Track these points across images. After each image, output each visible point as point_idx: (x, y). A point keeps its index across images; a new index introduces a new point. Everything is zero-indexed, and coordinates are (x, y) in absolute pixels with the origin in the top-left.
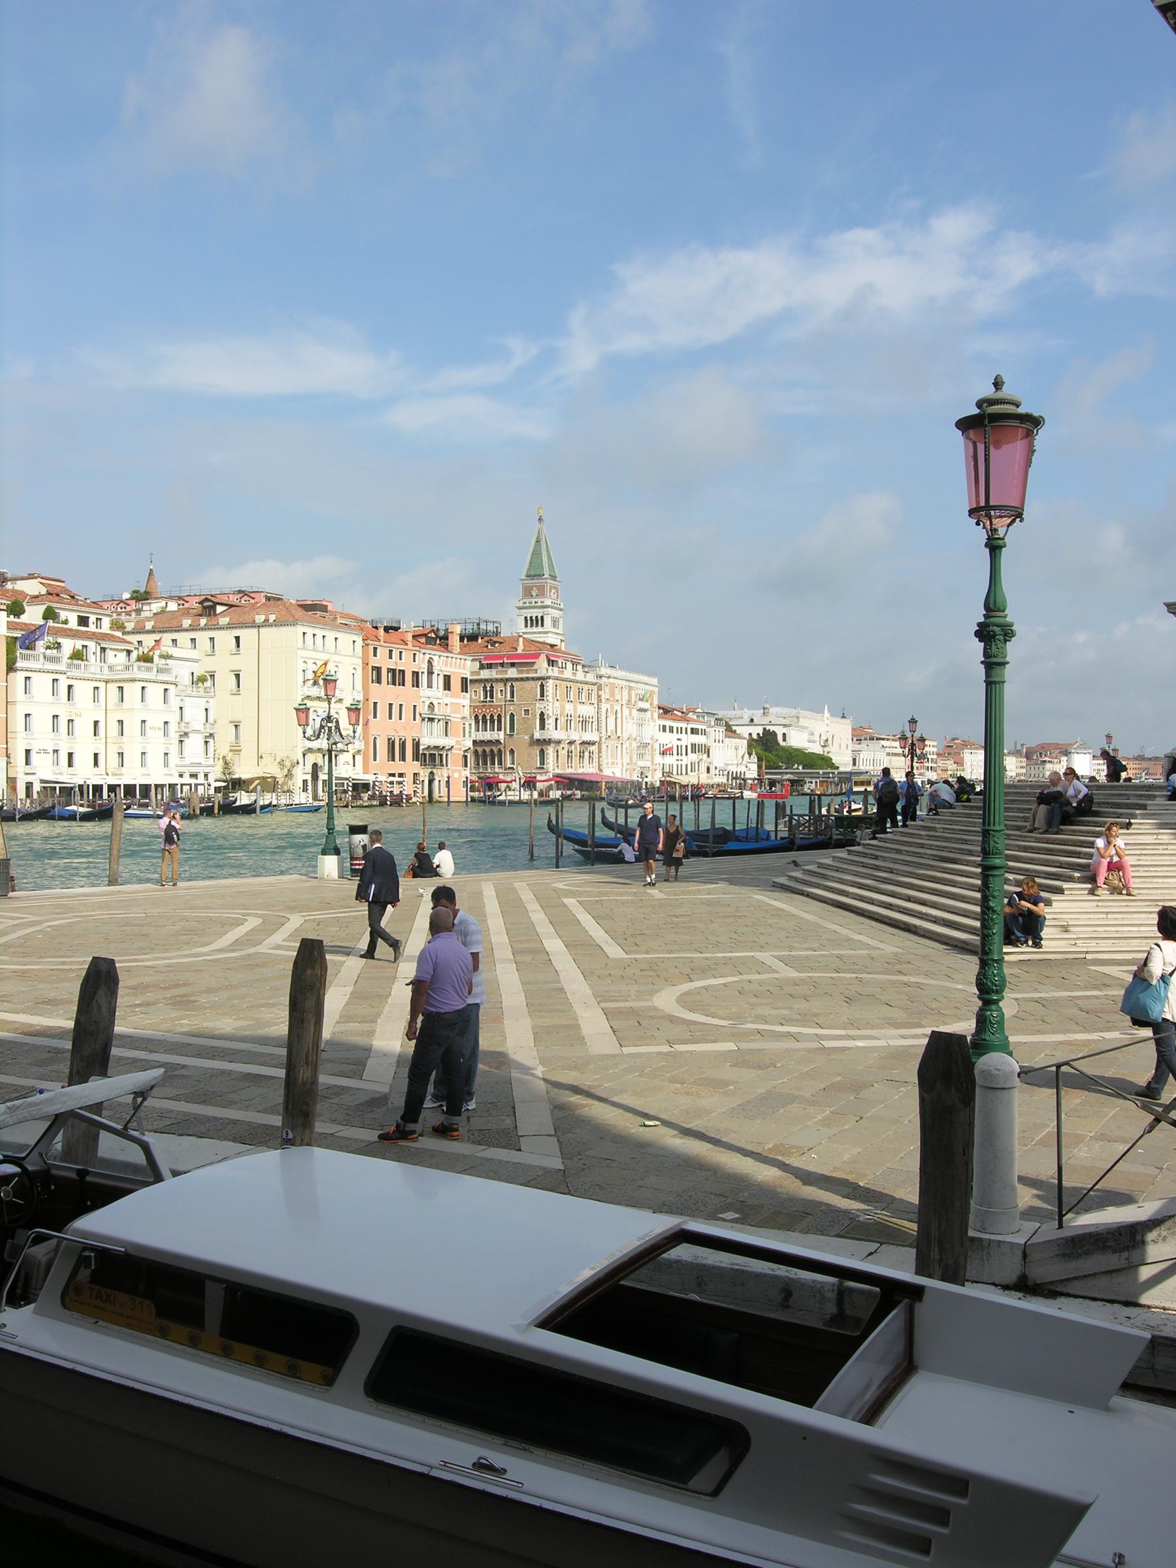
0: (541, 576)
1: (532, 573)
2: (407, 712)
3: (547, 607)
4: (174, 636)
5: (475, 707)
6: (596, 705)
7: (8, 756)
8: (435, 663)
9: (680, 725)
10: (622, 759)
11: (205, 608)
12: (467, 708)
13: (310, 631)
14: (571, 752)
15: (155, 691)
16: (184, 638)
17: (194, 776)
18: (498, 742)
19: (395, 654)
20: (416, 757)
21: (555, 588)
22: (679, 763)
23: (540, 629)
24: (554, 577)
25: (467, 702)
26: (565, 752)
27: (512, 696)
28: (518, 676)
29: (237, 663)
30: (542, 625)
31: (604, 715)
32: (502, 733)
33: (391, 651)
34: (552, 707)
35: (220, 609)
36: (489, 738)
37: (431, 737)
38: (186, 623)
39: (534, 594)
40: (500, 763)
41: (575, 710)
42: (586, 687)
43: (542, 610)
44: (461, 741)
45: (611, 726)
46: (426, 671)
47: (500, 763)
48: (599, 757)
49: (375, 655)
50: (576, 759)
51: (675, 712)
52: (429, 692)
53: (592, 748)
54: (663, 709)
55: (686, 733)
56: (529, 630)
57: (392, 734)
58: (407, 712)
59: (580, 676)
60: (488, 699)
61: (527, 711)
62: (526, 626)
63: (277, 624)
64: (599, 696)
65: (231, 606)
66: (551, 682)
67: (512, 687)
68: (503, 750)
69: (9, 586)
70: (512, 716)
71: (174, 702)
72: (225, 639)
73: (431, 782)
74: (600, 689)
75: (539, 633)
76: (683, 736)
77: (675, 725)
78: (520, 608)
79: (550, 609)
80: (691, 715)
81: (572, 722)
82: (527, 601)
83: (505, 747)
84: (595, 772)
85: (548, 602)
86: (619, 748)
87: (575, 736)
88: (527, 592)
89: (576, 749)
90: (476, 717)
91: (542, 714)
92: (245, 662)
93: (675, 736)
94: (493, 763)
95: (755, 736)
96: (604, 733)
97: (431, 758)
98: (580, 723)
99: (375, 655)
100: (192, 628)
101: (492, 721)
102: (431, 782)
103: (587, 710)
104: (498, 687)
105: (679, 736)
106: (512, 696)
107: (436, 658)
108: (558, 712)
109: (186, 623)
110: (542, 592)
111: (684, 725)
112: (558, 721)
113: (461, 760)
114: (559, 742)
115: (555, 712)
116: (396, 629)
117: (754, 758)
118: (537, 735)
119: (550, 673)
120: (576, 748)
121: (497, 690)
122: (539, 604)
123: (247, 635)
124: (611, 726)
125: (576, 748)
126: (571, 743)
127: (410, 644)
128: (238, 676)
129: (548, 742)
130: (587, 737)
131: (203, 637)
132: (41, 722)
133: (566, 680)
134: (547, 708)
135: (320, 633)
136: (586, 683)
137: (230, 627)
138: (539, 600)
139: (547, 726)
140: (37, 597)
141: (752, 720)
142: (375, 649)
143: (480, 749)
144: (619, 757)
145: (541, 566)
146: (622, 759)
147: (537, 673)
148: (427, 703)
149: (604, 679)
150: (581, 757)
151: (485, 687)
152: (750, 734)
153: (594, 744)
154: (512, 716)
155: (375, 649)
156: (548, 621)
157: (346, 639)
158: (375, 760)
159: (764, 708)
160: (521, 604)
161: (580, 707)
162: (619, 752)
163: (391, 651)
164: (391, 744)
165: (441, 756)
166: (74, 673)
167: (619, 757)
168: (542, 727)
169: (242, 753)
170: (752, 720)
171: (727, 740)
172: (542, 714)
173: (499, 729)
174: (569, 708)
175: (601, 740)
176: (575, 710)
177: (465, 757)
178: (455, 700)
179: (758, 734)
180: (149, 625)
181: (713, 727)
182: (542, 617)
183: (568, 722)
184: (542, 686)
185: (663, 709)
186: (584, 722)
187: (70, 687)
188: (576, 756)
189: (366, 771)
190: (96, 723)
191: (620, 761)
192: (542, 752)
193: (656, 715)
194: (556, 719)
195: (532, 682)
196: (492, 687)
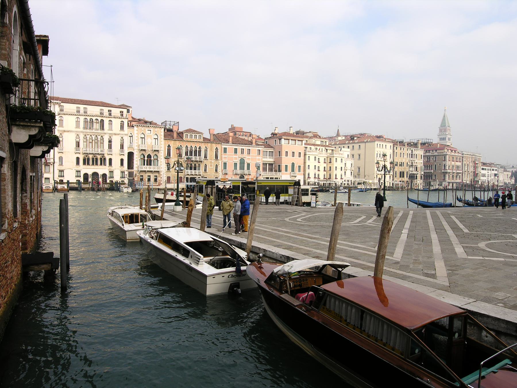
1: (442, 125)
2: (405, 164)
3: (447, 135)
4: (344, 146)
5: (424, 163)
7: (304, 175)
8: (413, 151)
9: (488, 168)
11: (351, 138)
12: (422, 163)
13: (379, 143)
15: (339, 160)
16: (346, 146)
17: (348, 181)
18: (431, 172)
19: (402, 149)
20: (407, 177)
22: (488, 179)
23: (444, 141)
24: (449, 127)
25: (422, 162)
26: (451, 176)
28: (438, 154)
29: (359, 152)
30: (445, 140)
31: (464, 165)
32: (432, 171)
33: (401, 148)
34: (448, 163)
35: (355, 138)
37: (412, 171)
38: (347, 142)
39: (443, 131)
40: (432, 179)
41: (455, 163)
42: (458, 157)
44: (420, 173)
45: (466, 169)
46: (411, 153)
47: (432, 179)
48: (462, 177)
49: (396, 149)
50: (455, 178)
52: (411, 159)
53: (460, 175)
55: (491, 170)
56: (441, 141)
57: (401, 170)
58: (405, 164)
59: (456, 154)
61: (440, 164)
62: (440, 140)
63: (370, 142)
64: (462, 160)
65: (358, 138)
66: (448, 156)
67: (436, 157)
69: (305, 135)
71: (344, 162)
72: (356, 146)
73: (411, 183)
74: (463, 157)
76: (490, 171)
77: (487, 168)
78: (438, 135)
80: (492, 165)
86: (469, 175)
87: (454, 171)
88: (441, 131)
89: (455, 175)
90: (425, 166)
92: (362, 152)
93: (487, 171)
94: (429, 179)
95: (514, 171)
96: (464, 170)
97: (412, 177)
99: (396, 149)
100: (348, 143)
101: (430, 167)
102: (411, 183)
103: (459, 164)
104: (431, 158)
105: (488, 171)
107: (413, 150)
109: (347, 142)
110: (445, 130)
111: (490, 168)
113: (420, 177)
114: (450, 173)
116: (402, 142)
117: (514, 178)
118: (443, 171)
119: (447, 153)
120: (455, 174)
123: (362, 145)
124: (466, 169)
125: (455, 174)
126: (453, 173)
127: (406, 146)
128: (359, 155)
129: (447, 173)
130: (458, 171)
131: (351, 146)
132: (312, 167)
133: (452, 155)
135: (381, 144)
136: (459, 156)
137: (358, 143)
139: (446, 168)
140: (311, 137)
141: (513, 167)
142: (397, 148)
143: (426, 175)
144: (469, 177)
145: (445, 123)
148: (411, 162)
149: (464, 155)
150: (457, 177)
151: (427, 158)
152: (512, 171)
153: (461, 173)
155: (397, 148)
156: (447, 139)
157: (389, 145)
158: (396, 177)
160: (439, 134)
161: (456, 163)
162: (469, 176)
163: (401, 148)
164: (400, 172)
165: (414, 176)
166: (320, 155)
167: (469, 177)
168: (445, 169)
169: (360, 175)
170: (513, 167)
171: (505, 173)
173: (432, 169)
174: (453, 163)
175: (463, 172)
176: (455, 163)
177: (421, 177)
178: (419, 161)
180: (338, 143)
183: (453, 167)
184: (445, 157)
186: (458, 167)
187: (319, 158)
189: (393, 180)
190: (325, 167)
191: (469, 178)
192: (444, 176)
193: (481, 165)
194: (449, 166)
195: (442, 156)
196: (430, 157)
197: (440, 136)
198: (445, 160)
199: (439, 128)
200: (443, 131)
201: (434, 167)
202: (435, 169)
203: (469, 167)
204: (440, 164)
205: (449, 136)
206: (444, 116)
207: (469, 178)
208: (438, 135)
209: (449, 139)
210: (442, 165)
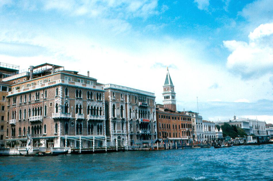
6: (104, 102)
10: (127, 129)
14: (81, 125)
23: (168, 99)
27: (46, 97)
30: (169, 98)
36: (37, 119)
39: (167, 90)
56: (165, 100)
60: (38, 99)
61: (51, 104)
62: (165, 99)
68: (42, 125)
70: (46, 106)
75: (169, 100)
78: (163, 94)
81: (82, 110)
82: (165, 92)
83: (43, 124)
106: (46, 97)
121: (41, 94)
138: (168, 91)
146: (127, 129)
147: (55, 83)
153: (101, 121)
154: (46, 106)
159: (234, 117)
160: (163, 93)
182: (169, 96)
188: (85, 127)
191: (125, 131)
197: (164, 95)
198: (56, 97)
199: (163, 87)
200: (167, 90)
201: (43, 110)
202: (46, 115)
203: (124, 111)
204: (51, 104)
207: (125, 131)
210: (54, 105)
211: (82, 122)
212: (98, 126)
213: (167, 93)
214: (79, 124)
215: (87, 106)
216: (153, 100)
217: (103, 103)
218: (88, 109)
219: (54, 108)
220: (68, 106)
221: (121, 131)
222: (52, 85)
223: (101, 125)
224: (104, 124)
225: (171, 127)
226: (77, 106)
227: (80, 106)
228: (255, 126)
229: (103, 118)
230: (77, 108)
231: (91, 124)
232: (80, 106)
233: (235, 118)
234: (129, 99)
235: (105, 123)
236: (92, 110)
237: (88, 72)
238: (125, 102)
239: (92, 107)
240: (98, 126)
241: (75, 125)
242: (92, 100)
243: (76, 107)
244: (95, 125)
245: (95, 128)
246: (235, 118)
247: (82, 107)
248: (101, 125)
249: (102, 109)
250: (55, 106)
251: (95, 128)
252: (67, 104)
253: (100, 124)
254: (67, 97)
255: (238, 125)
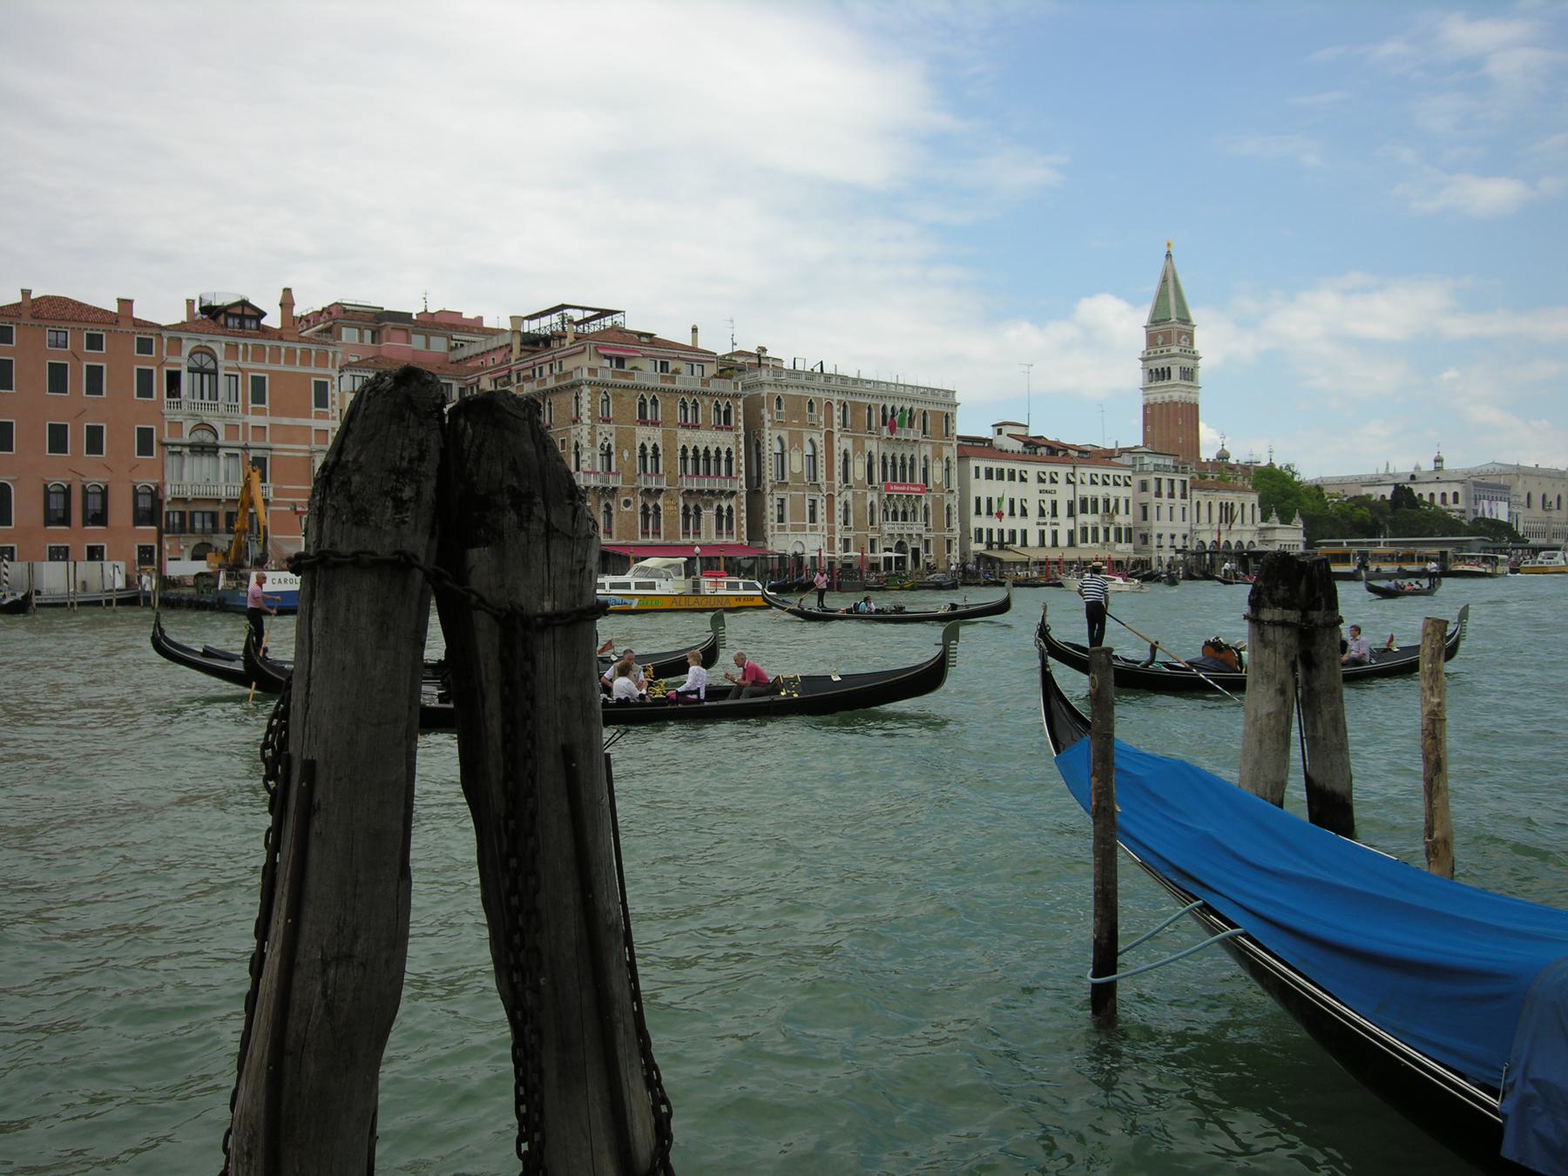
0: (1166, 320)
1: (1157, 318)
21: (1187, 334)
23: (1165, 383)
24: (1186, 321)
30: (1169, 377)
41: (669, 438)
43: (1168, 360)
51: (1070, 451)
54: (1049, 447)
56: (1152, 385)
61: (563, 441)
79: (1177, 359)
84: (733, 541)
85: (1175, 350)
88: (1152, 340)
91: (577, 446)
98: (690, 462)
108: (612, 441)
112: (613, 458)
115: (600, 440)
122: (1165, 353)
134: (582, 434)
156: (1175, 373)
159: (1436, 461)
160: (1145, 356)
171: (1196, 495)
172: (577, 446)
176: (669, 438)
179: (1383, 496)
181: (1152, 472)
182: (1169, 368)
185: (1049, 447)
197: (1150, 362)
198: (575, 422)
205: (1188, 363)
206: (1165, 281)
208: (1143, 360)
209: (1188, 374)
211: (662, 496)
212: (719, 509)
213: (1160, 358)
214: (651, 505)
215: (680, 447)
216: (947, 416)
217: (737, 436)
218: (684, 458)
219: (570, 456)
220: (613, 449)
221: (804, 526)
222: (563, 383)
223: (730, 509)
224: (742, 504)
225: (1059, 512)
226: (643, 447)
227: (655, 448)
228: (1544, 497)
229: (740, 485)
230: (643, 456)
231: (691, 506)
232: (655, 448)
233: (1438, 465)
234: (839, 417)
235: (744, 500)
236: (696, 458)
237: (695, 330)
238: (823, 426)
239: (696, 450)
240: (719, 509)
241: (635, 508)
242: (696, 427)
243: (638, 451)
244: (709, 504)
245: (708, 515)
246: (1438, 465)
247: (661, 452)
248: (730, 509)
249: (734, 456)
250: (573, 450)
251: (708, 515)
252: (606, 444)
253: (725, 506)
254: (607, 421)
255: (1432, 495)
